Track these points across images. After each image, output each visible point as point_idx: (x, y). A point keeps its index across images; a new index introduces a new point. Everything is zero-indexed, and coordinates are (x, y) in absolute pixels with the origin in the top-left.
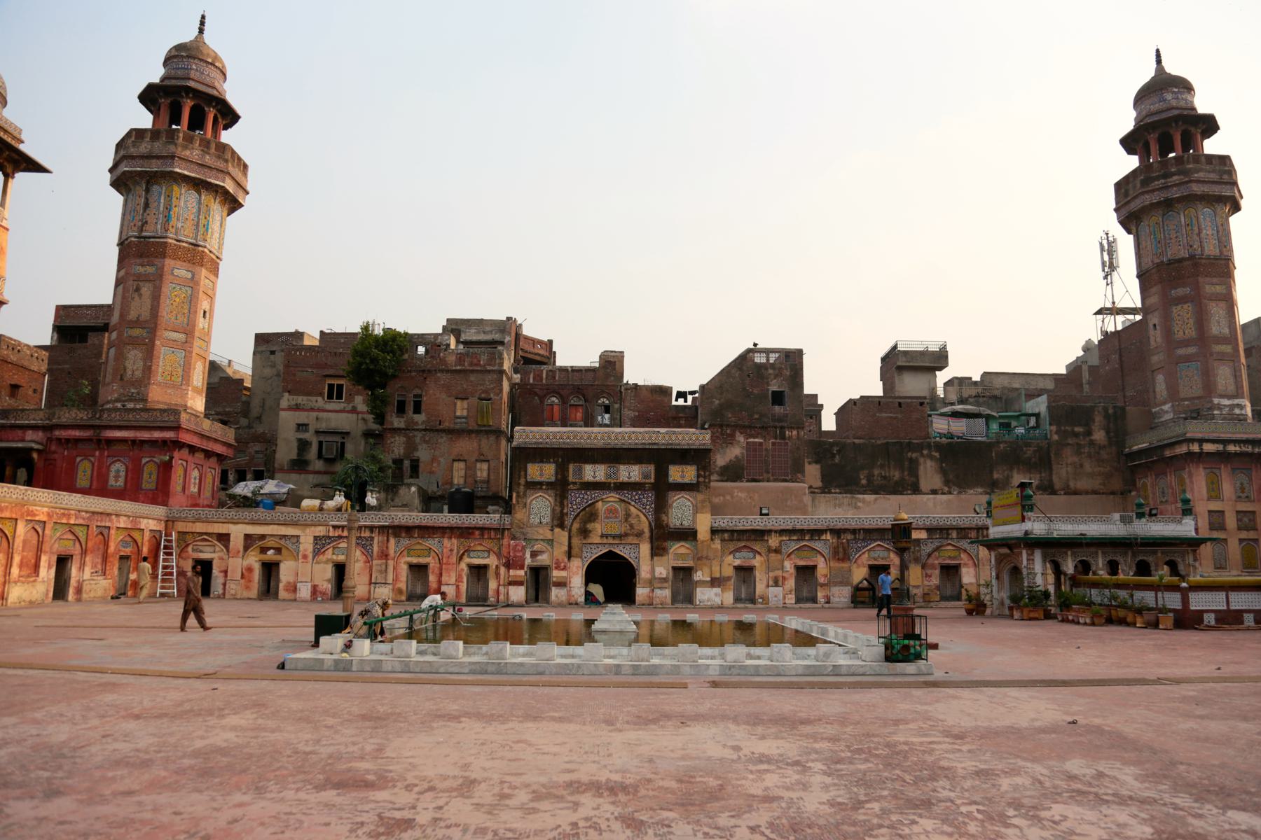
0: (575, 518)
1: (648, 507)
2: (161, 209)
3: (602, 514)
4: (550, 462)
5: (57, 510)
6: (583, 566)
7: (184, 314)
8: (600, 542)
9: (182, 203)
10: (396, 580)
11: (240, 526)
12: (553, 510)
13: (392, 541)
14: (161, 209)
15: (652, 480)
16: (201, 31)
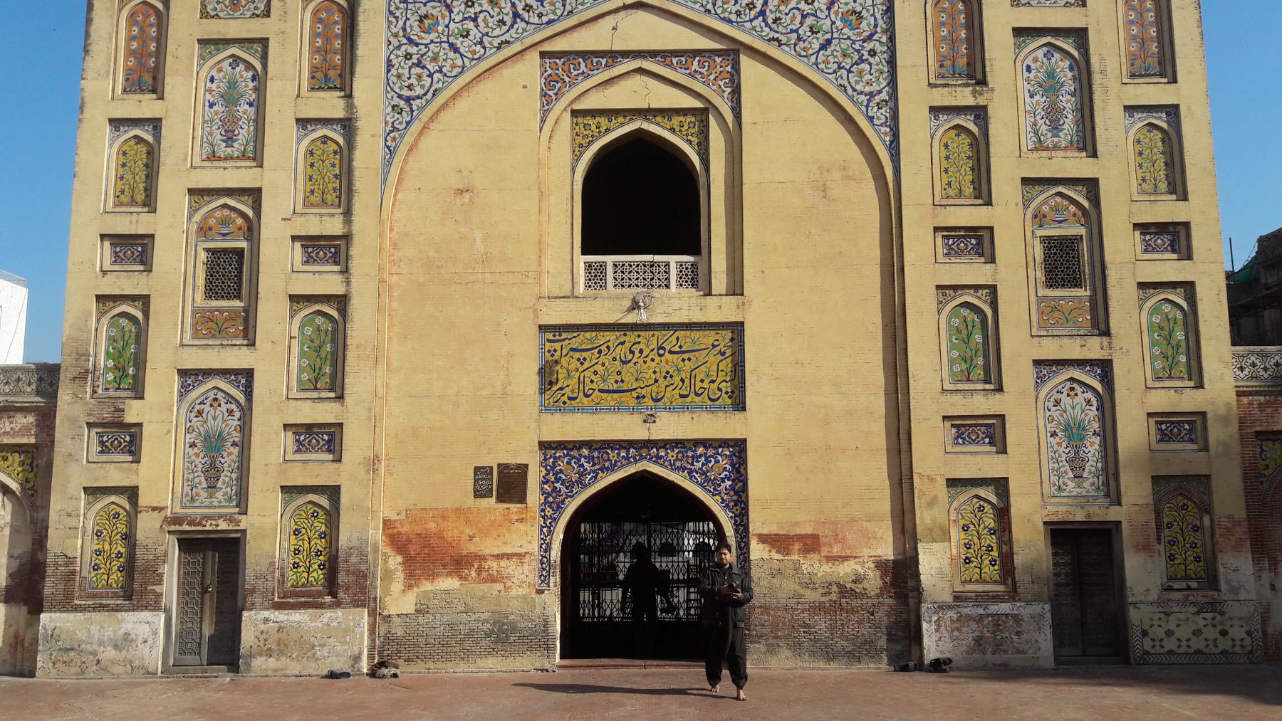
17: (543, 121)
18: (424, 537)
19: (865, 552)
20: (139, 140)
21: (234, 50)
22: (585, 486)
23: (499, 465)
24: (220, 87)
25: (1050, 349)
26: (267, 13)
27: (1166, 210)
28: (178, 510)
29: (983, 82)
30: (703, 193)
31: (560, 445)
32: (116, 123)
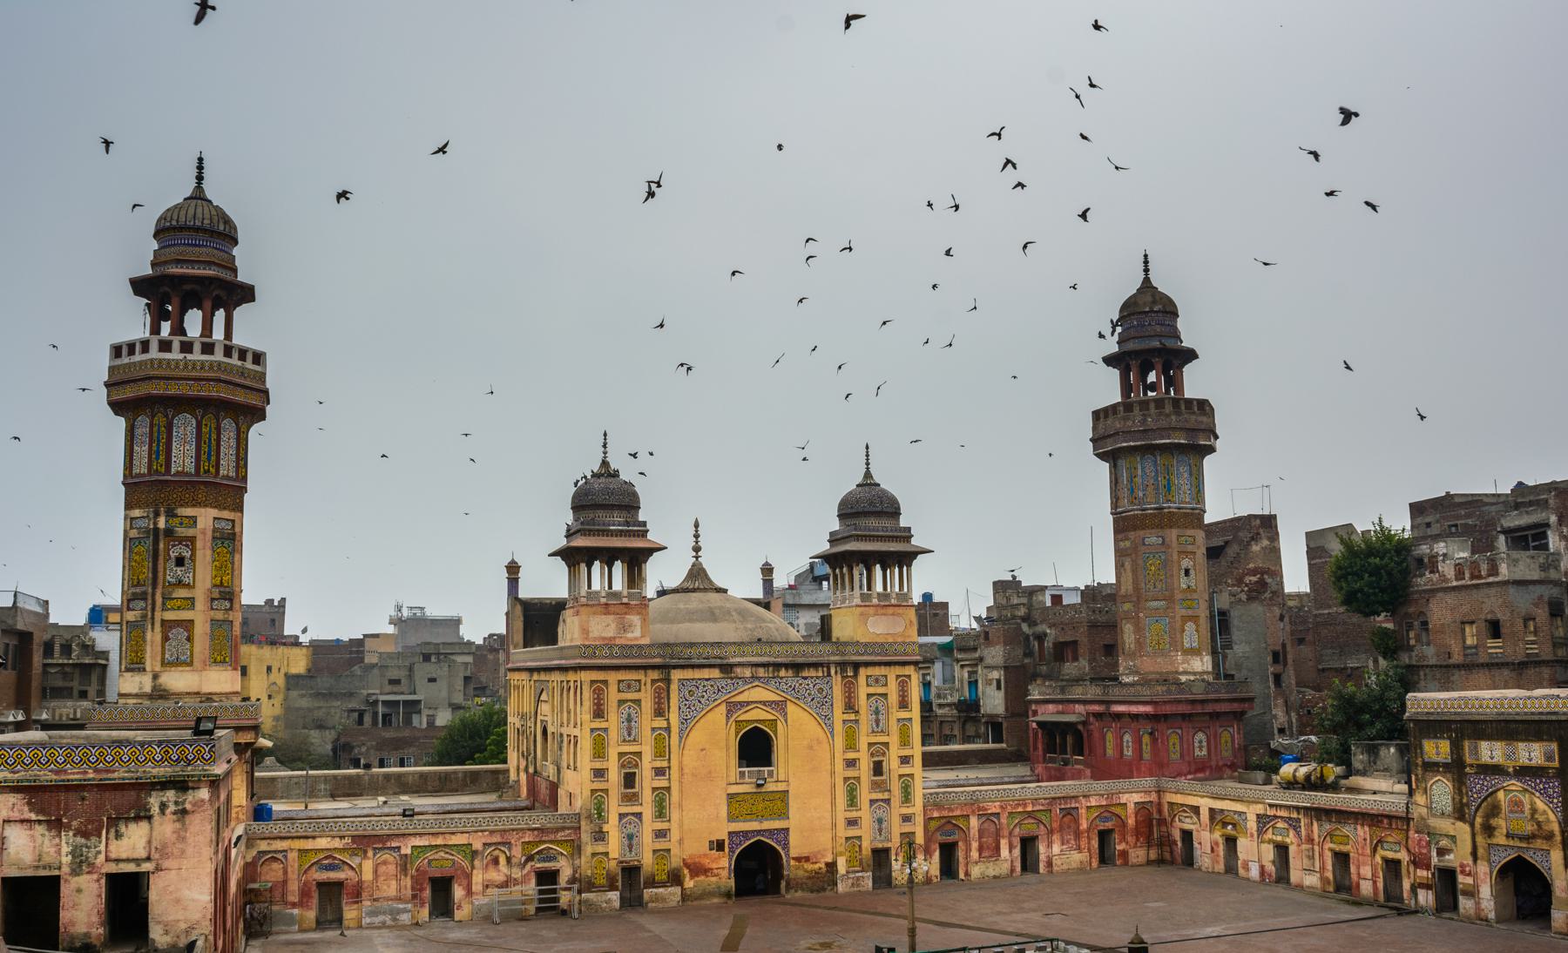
0: (1477, 809)
1: (1555, 801)
2: (1125, 482)
3: (1504, 806)
4: (1444, 738)
5: (1011, 803)
6: (1491, 873)
7: (1161, 580)
8: (1506, 843)
9: (1139, 472)
10: (1323, 868)
11: (1206, 799)
12: (1453, 799)
13: (1315, 824)
14: (1125, 482)
15: (1556, 764)
16: (1146, 270)
17: (727, 725)
18: (695, 863)
19: (823, 860)
20: (599, 735)
21: (629, 703)
22: (741, 845)
23: (717, 841)
24: (624, 716)
25: (875, 796)
26: (640, 690)
27: (906, 752)
28: (621, 859)
29: (858, 712)
30: (775, 747)
31: (734, 832)
32: (592, 730)
